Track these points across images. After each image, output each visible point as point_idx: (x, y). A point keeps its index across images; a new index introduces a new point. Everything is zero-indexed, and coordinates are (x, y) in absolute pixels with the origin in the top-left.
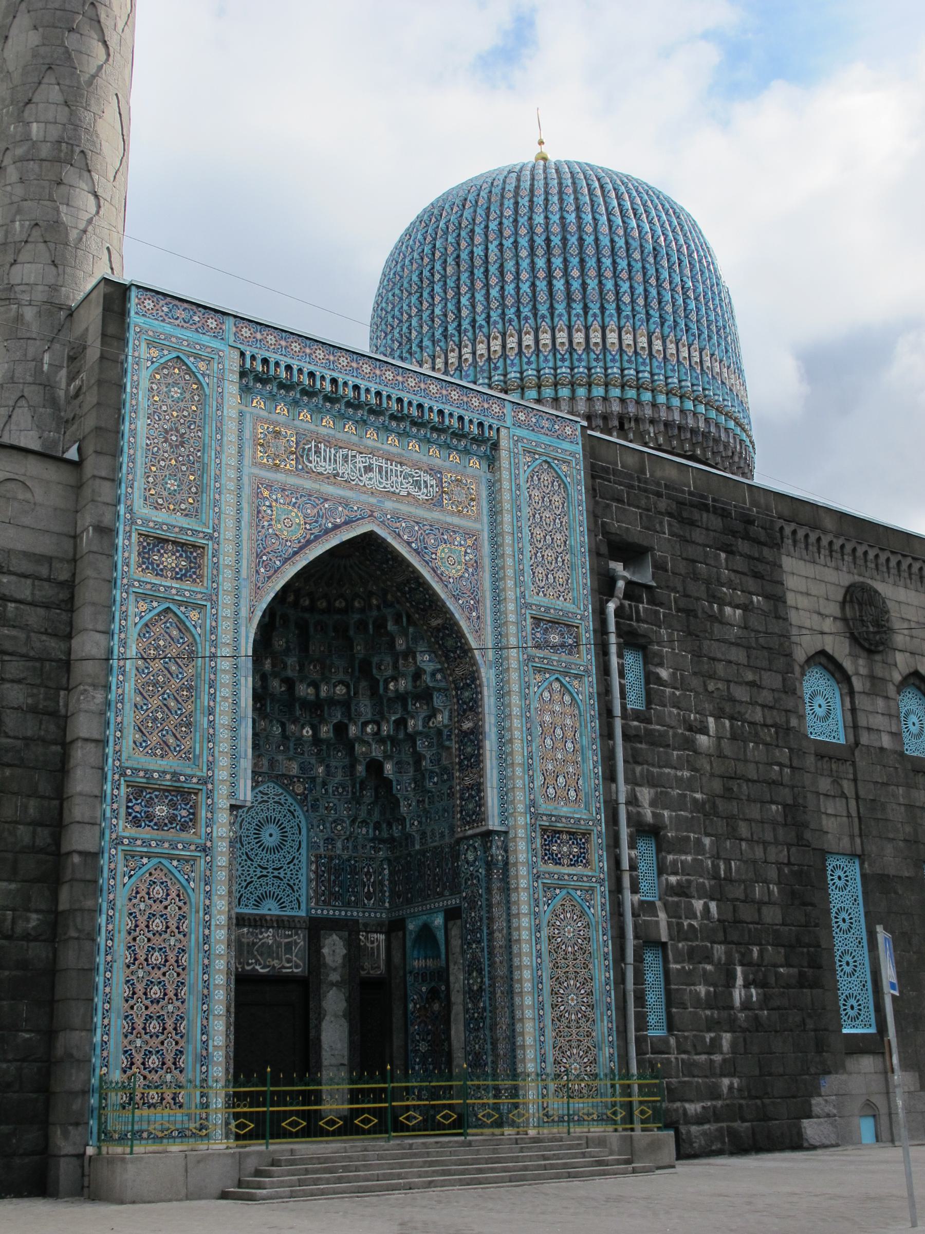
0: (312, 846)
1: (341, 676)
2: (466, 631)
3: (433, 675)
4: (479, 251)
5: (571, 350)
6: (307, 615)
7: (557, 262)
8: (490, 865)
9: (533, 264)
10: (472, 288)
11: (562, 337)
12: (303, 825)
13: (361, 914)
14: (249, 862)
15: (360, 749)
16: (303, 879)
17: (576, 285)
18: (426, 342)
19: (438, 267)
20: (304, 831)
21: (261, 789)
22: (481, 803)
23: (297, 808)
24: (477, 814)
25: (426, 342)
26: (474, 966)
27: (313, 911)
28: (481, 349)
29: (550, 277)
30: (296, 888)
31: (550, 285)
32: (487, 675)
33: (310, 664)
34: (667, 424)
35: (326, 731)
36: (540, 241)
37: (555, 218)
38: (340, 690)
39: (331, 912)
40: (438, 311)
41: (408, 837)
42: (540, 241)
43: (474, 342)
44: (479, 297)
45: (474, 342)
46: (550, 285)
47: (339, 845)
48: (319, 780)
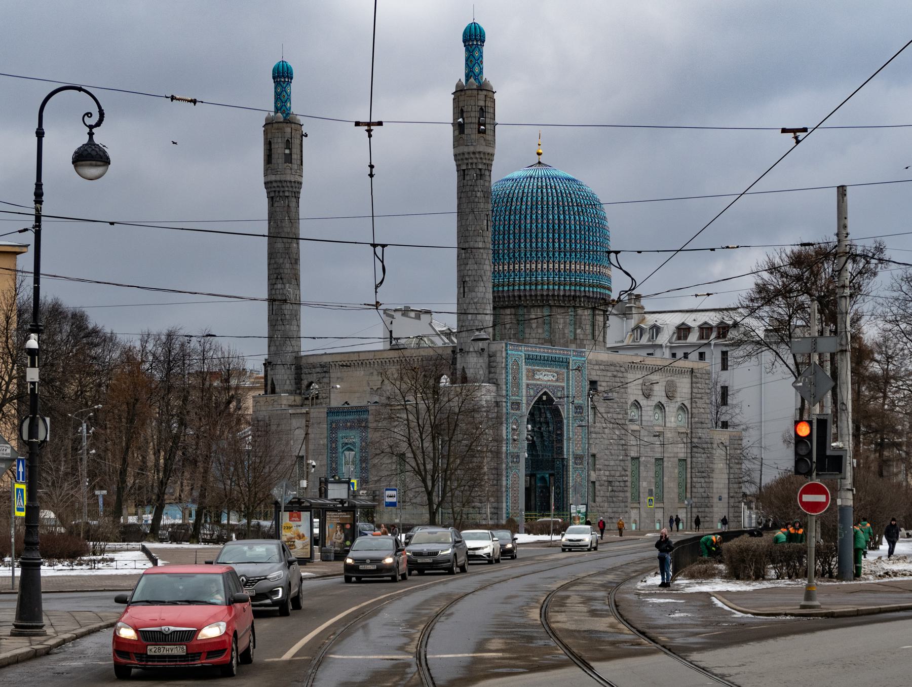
4: (528, 226)
5: (559, 271)
7: (557, 236)
8: (563, 466)
9: (548, 236)
10: (525, 241)
11: (557, 266)
17: (562, 246)
18: (506, 257)
19: (512, 228)
22: (563, 451)
24: (562, 453)
25: (506, 257)
26: (557, 488)
28: (528, 266)
29: (554, 242)
31: (553, 245)
32: (565, 421)
34: (589, 297)
36: (551, 226)
37: (556, 217)
40: (511, 246)
41: (538, 455)
42: (551, 226)
43: (525, 262)
44: (528, 245)
45: (525, 262)
46: (553, 245)
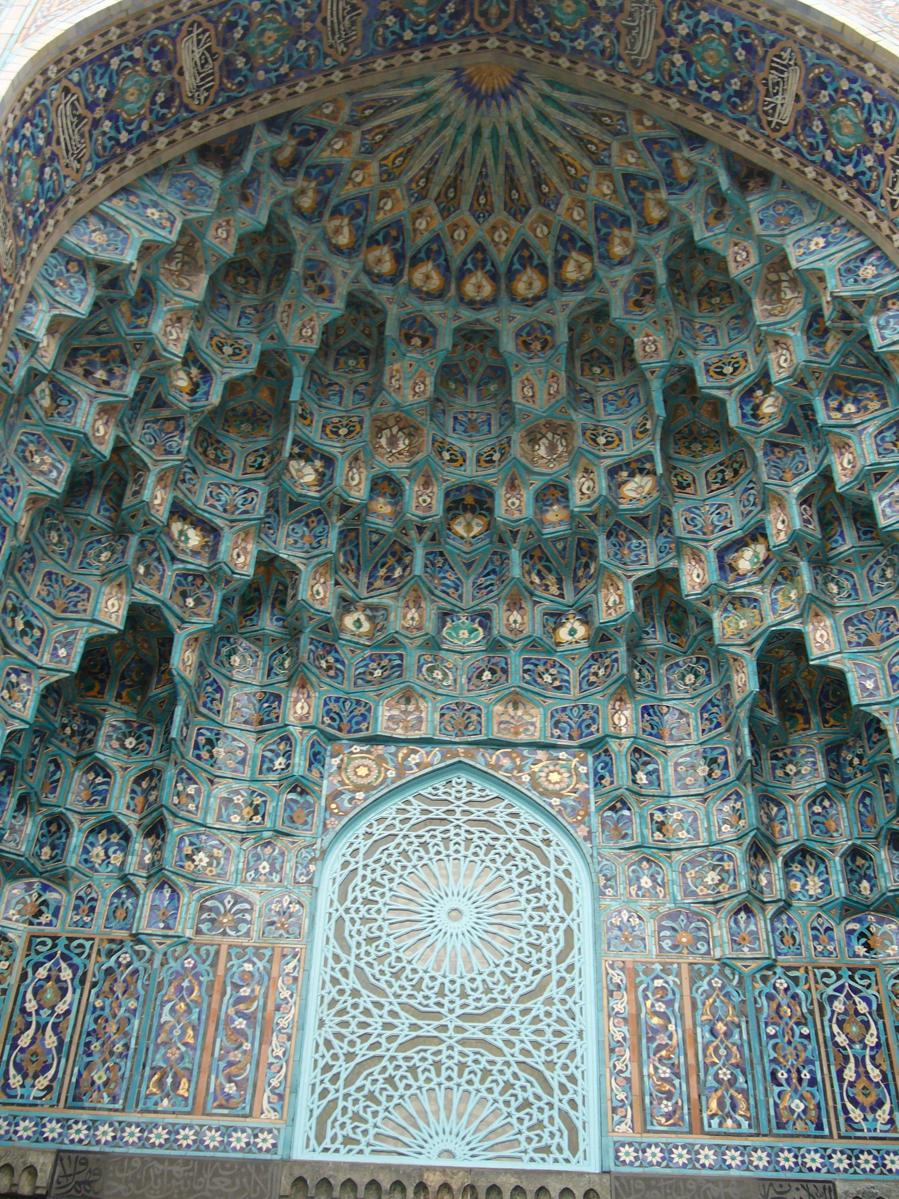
0: (615, 936)
1: (628, 448)
2: (863, 32)
3: (849, 271)
6: (488, 316)
12: (581, 882)
13: (840, 1162)
14: (366, 999)
15: (728, 626)
16: (589, 1049)
20: (584, 900)
21: (426, 790)
23: (555, 834)
27: (627, 1154)
30: (556, 1077)
33: (533, 438)
35: (616, 602)
38: (637, 490)
39: (708, 1157)
47: (720, 929)
48: (620, 749)
